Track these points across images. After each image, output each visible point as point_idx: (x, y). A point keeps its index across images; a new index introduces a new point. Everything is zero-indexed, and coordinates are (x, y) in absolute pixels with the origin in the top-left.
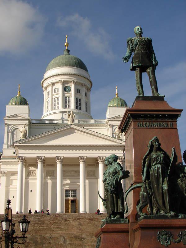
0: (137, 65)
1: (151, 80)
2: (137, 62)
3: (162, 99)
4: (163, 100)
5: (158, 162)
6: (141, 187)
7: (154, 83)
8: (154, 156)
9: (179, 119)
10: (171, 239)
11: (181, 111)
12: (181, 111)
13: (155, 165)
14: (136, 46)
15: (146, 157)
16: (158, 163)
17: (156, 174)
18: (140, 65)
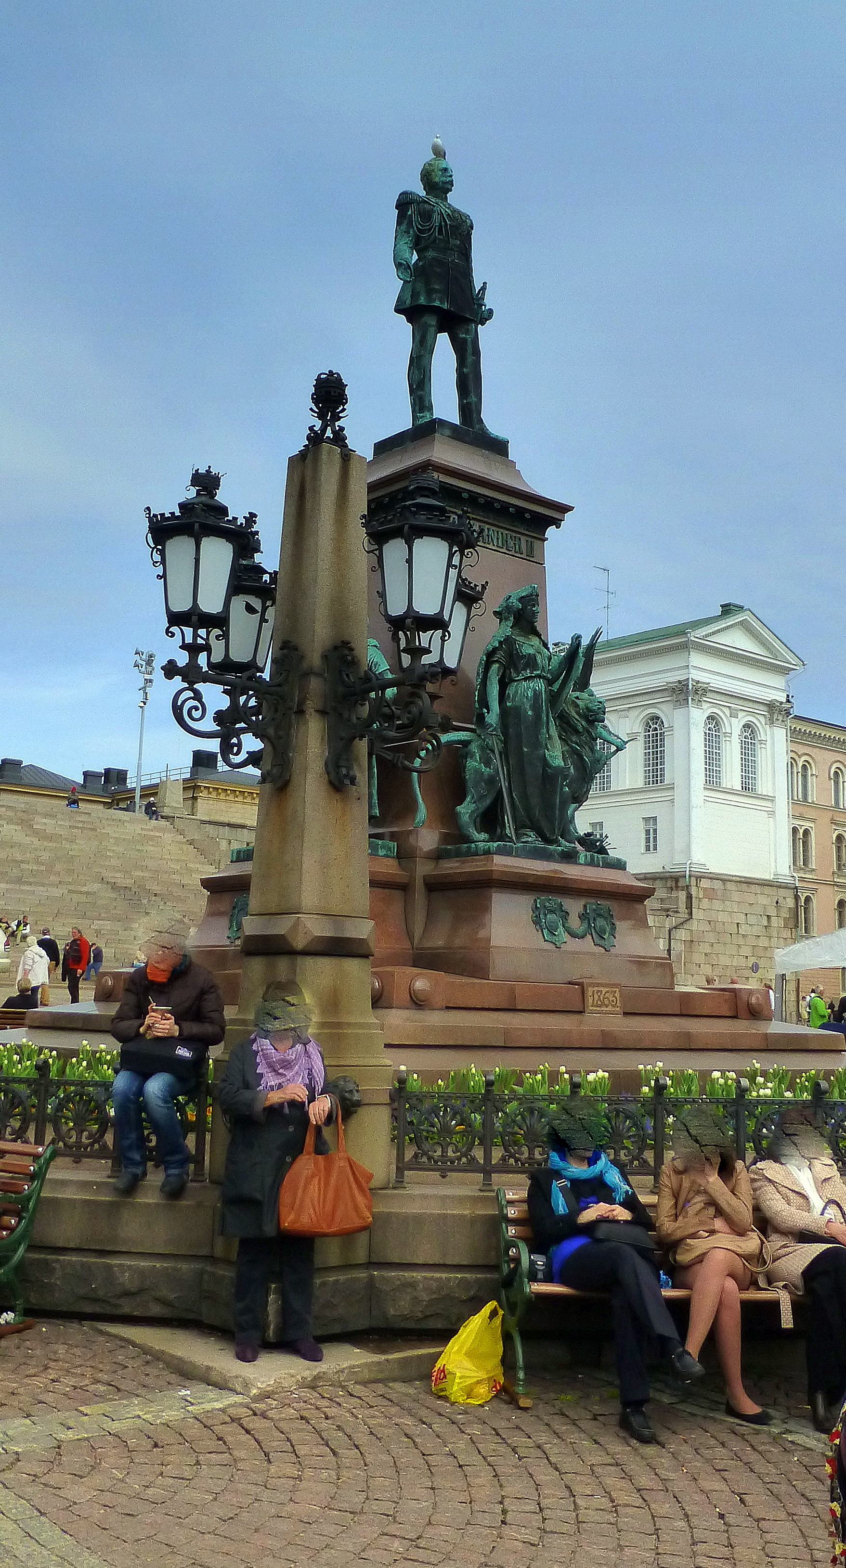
0: (437, 303)
1: (465, 370)
2: (436, 291)
3: (499, 447)
4: (506, 455)
5: (539, 672)
6: (466, 743)
7: (469, 383)
8: (527, 650)
9: (551, 531)
10: (567, 925)
11: (565, 509)
12: (565, 509)
13: (525, 679)
14: (440, 233)
15: (495, 650)
16: (539, 676)
17: (530, 713)
18: (445, 306)
